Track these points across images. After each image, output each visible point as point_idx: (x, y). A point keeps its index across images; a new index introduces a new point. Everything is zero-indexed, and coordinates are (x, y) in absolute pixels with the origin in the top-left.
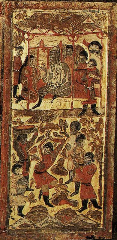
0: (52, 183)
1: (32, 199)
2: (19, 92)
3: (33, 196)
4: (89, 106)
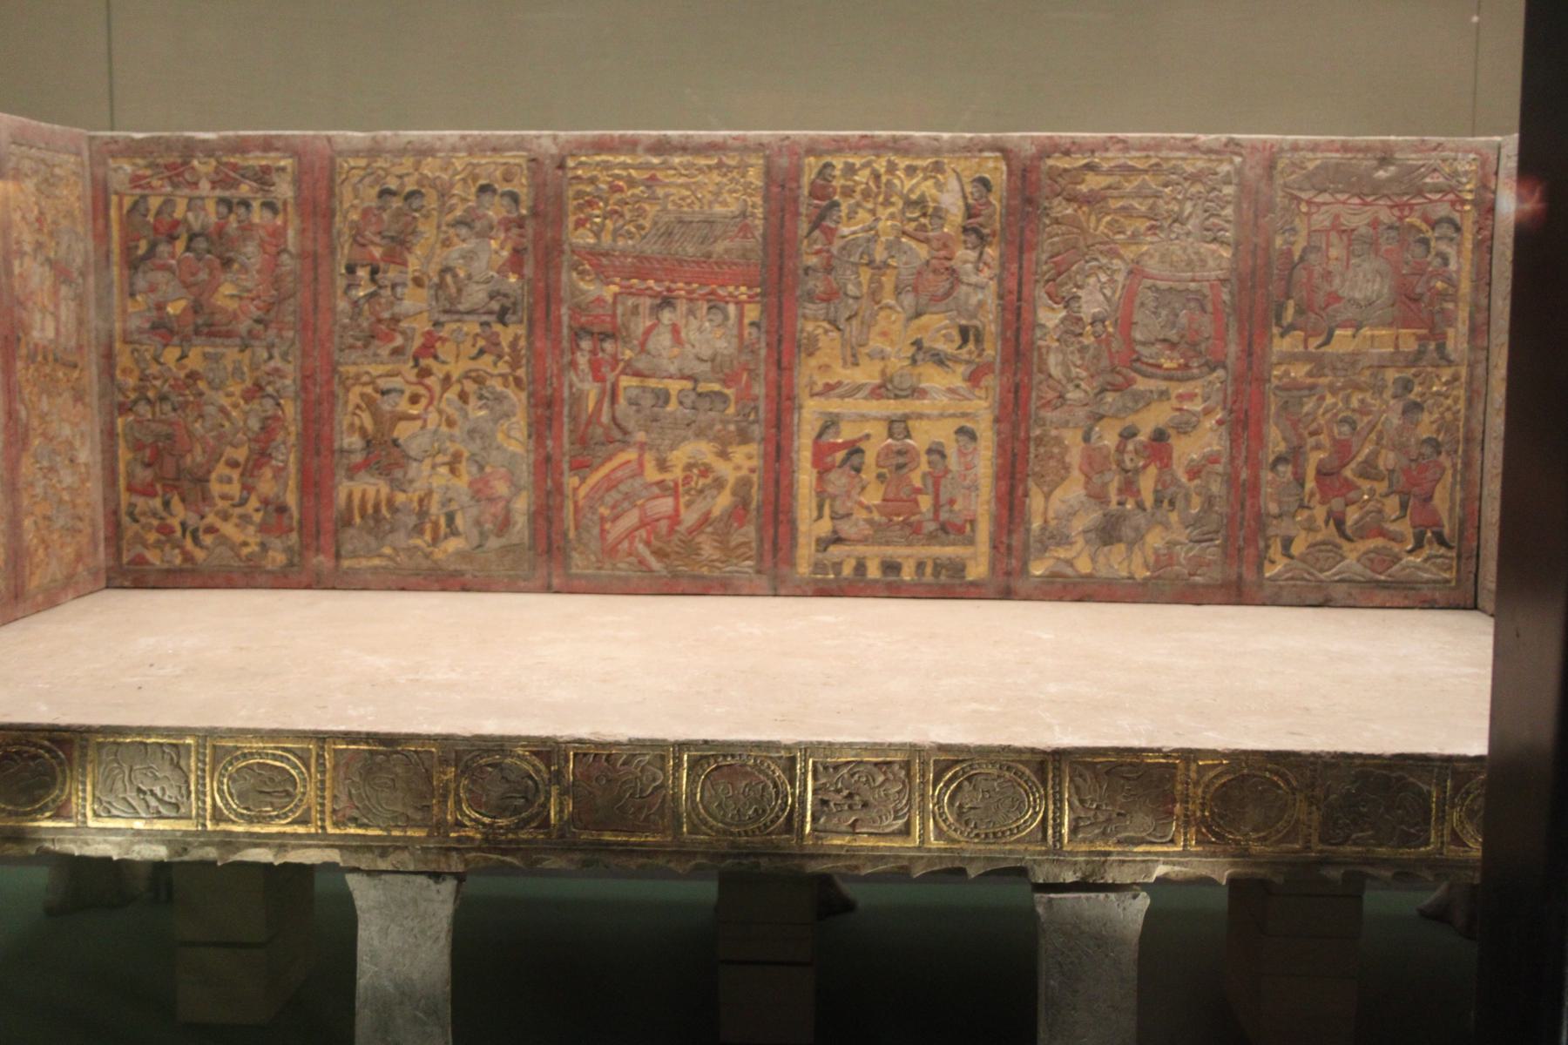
0: (1352, 495)
1: (1310, 528)
2: (1289, 315)
3: (1311, 519)
4: (1432, 346)
